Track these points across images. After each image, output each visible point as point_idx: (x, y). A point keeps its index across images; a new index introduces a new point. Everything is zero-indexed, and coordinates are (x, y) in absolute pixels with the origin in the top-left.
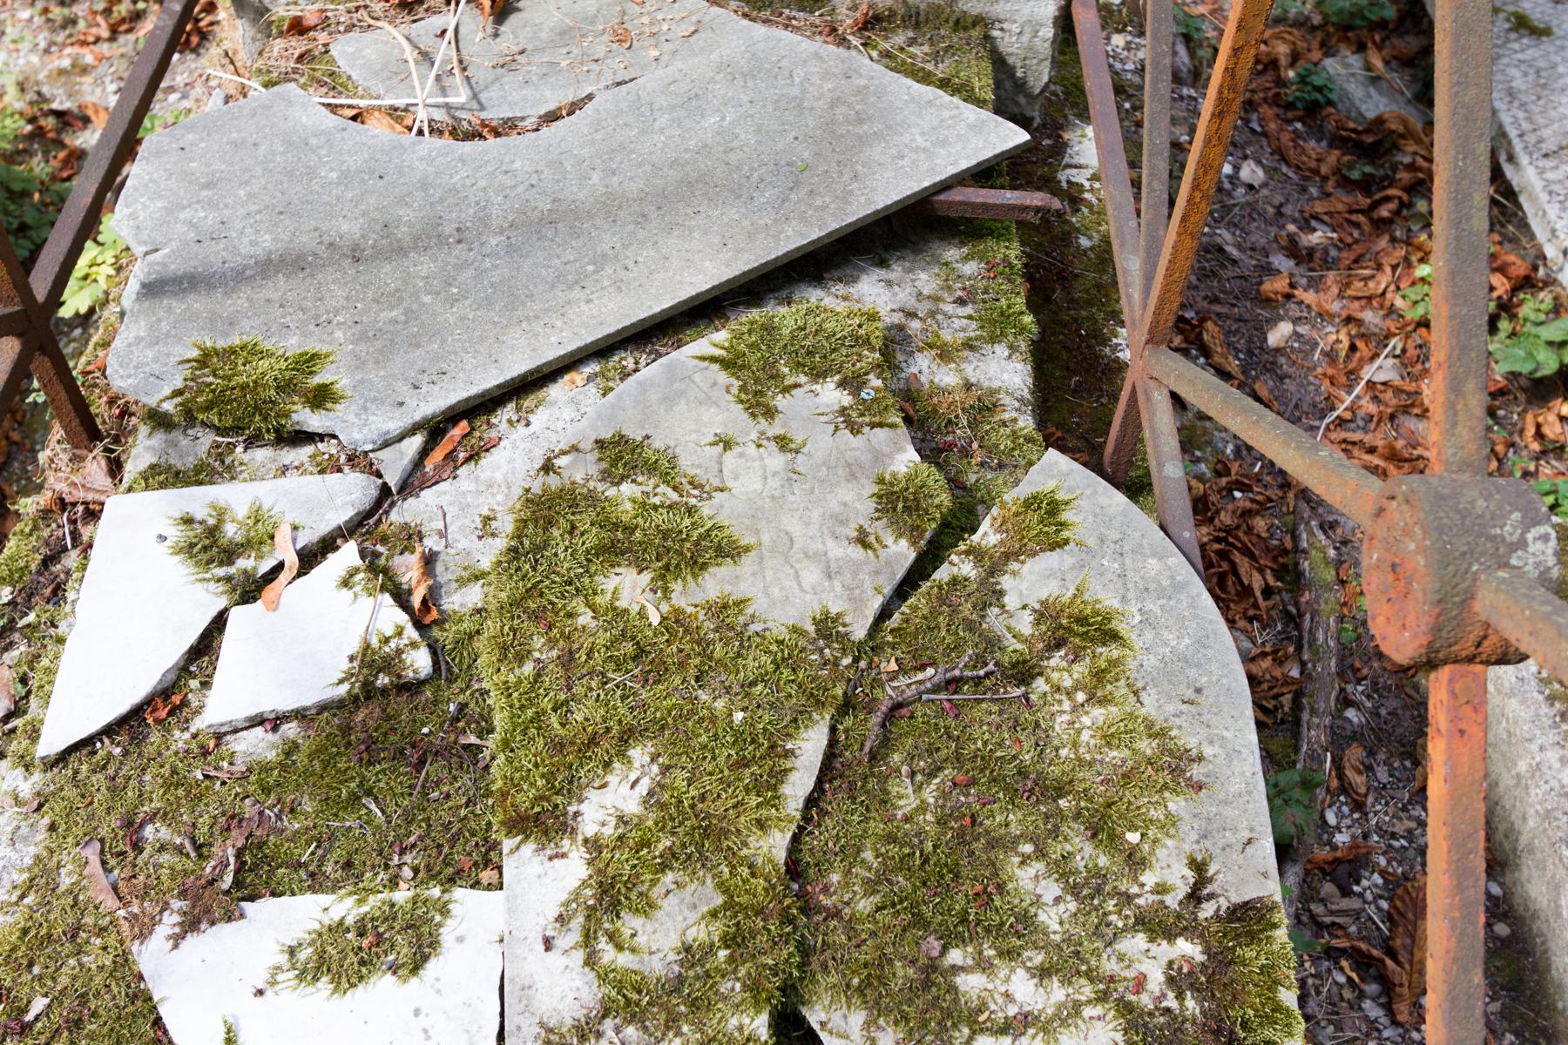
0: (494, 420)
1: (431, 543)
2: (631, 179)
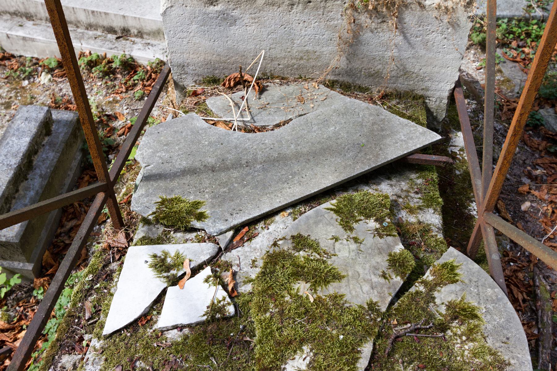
0: (257, 227)
1: (235, 268)
2: (304, 147)
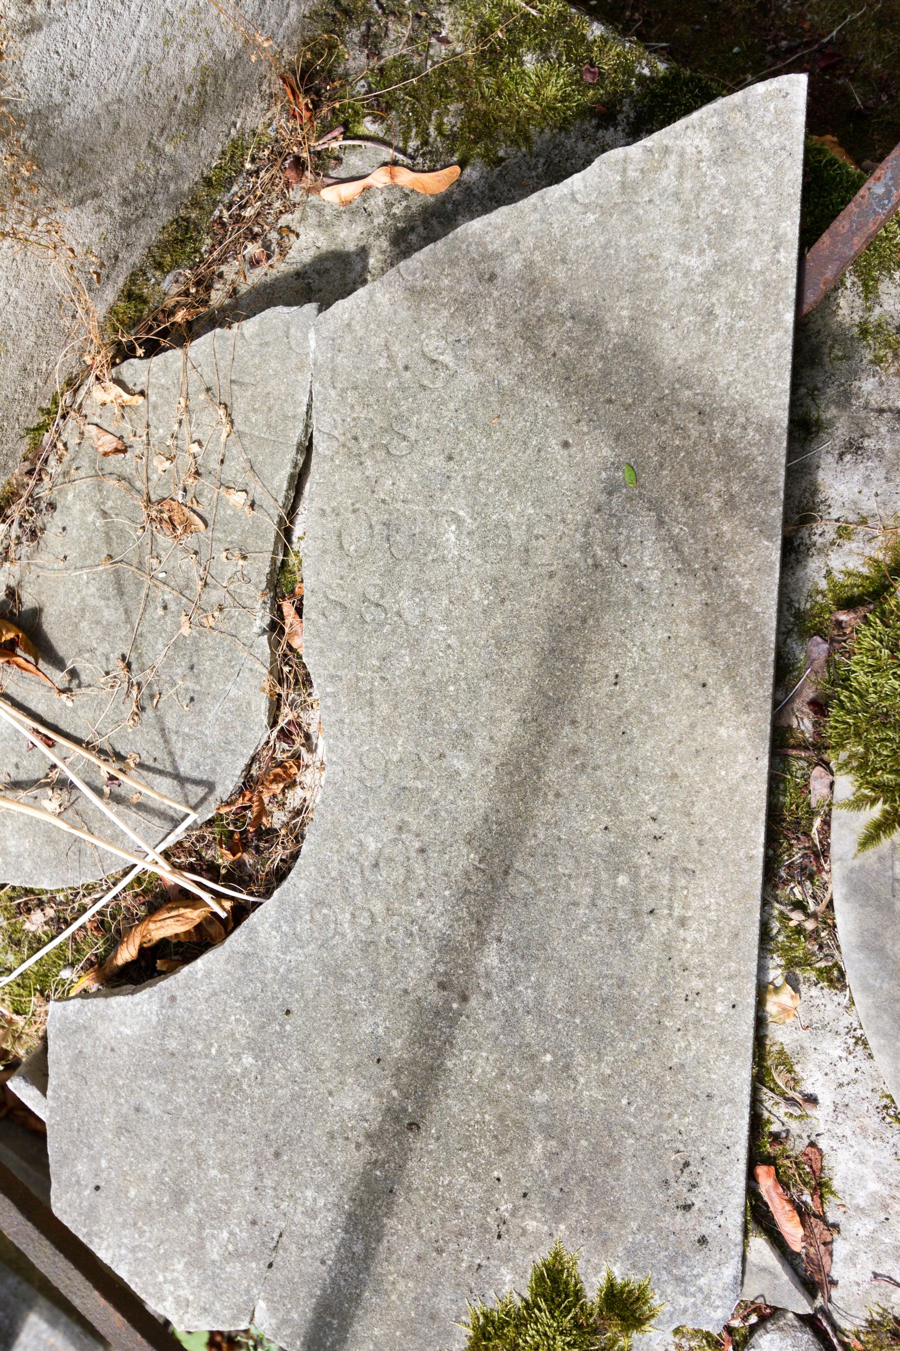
0: (775, 1128)
2: (492, 720)
